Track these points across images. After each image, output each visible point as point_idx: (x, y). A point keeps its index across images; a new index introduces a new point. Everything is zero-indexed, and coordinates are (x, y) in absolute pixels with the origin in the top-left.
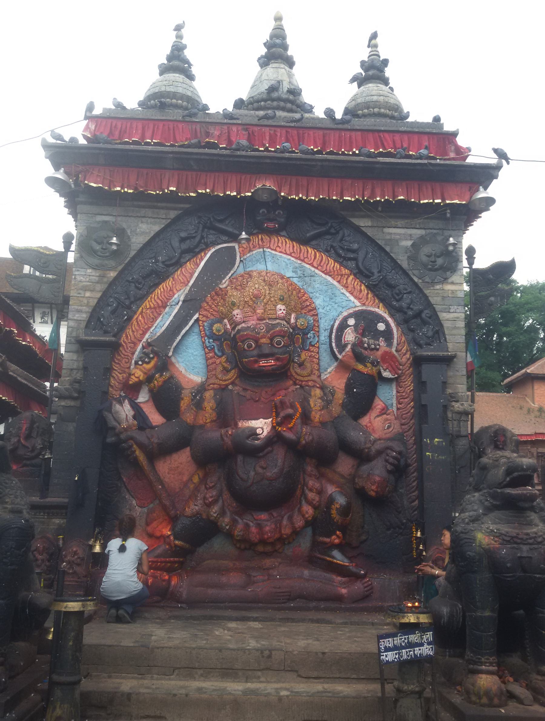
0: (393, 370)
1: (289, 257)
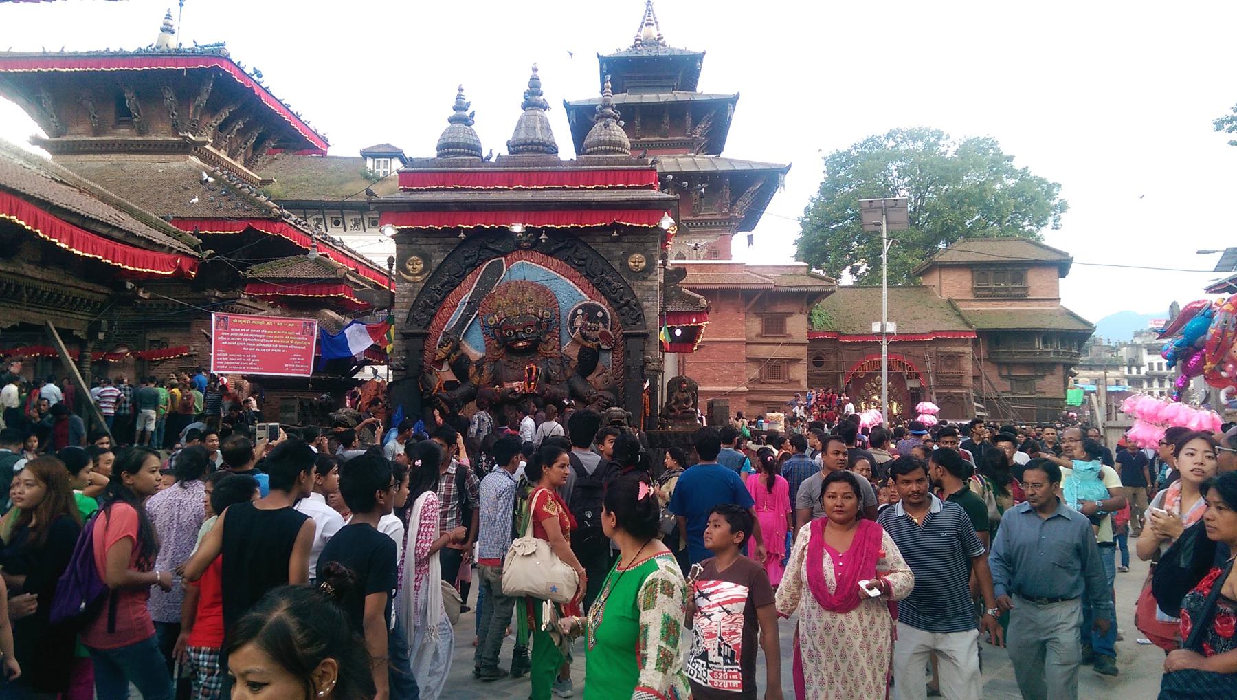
0: (608, 343)
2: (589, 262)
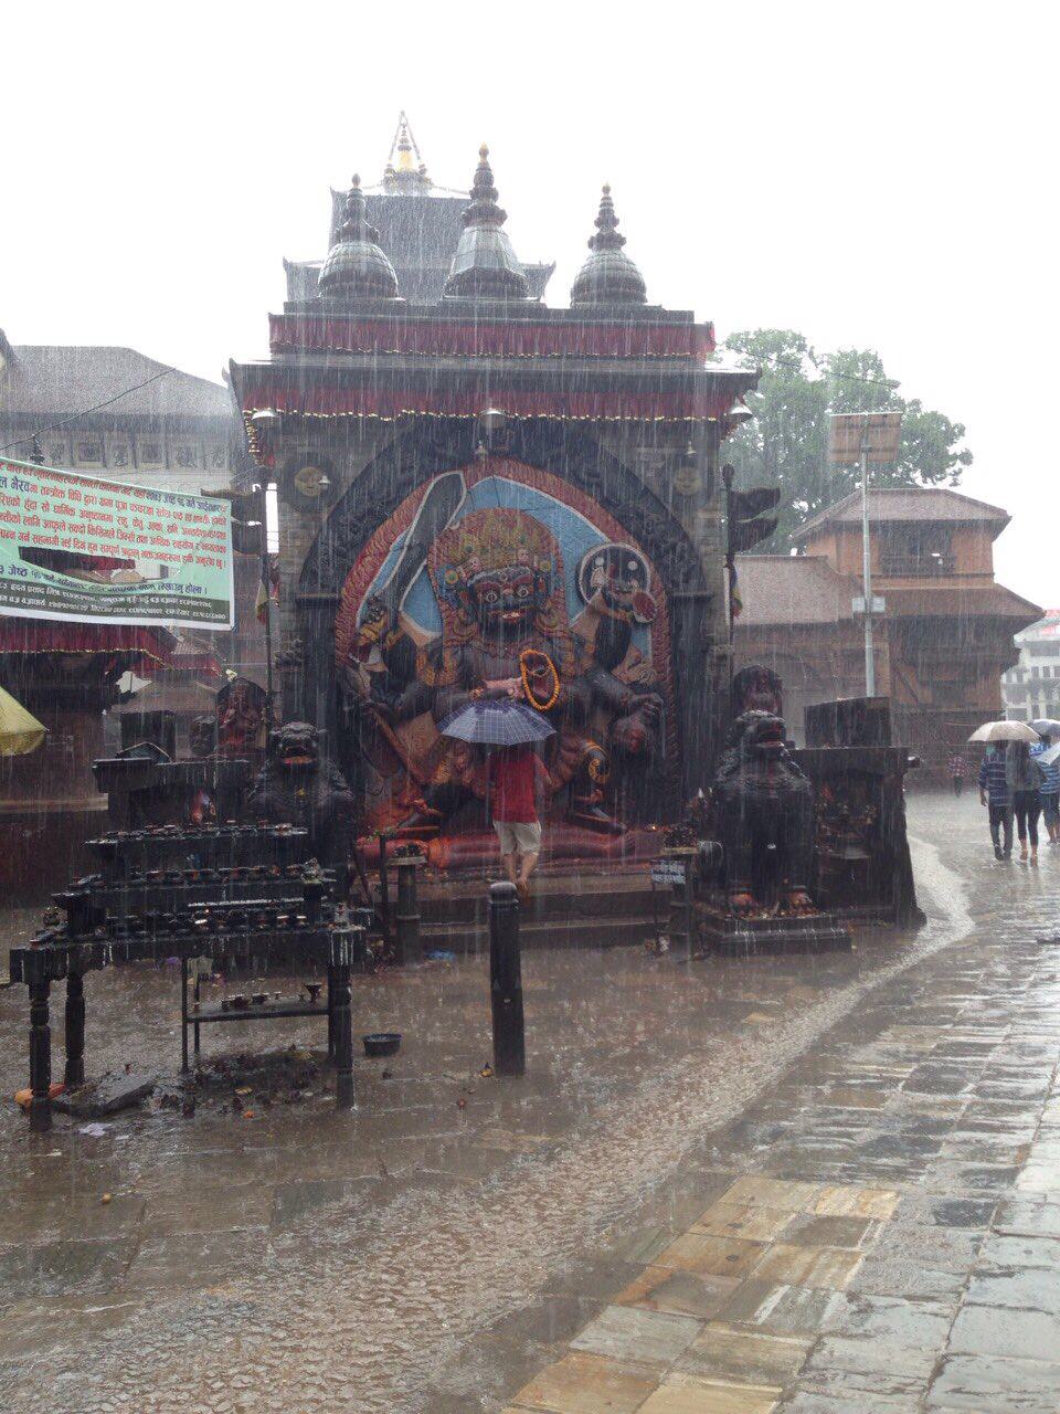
0: (648, 615)
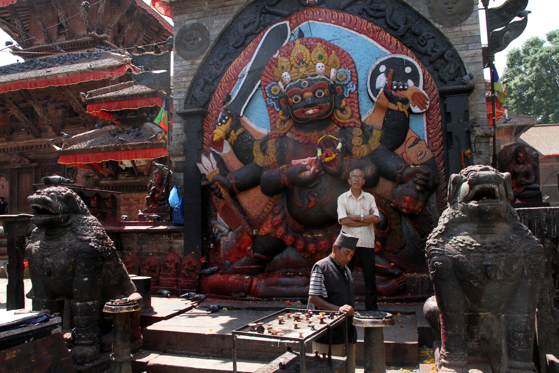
0: (422, 106)
1: (329, 24)
2: (388, 13)
